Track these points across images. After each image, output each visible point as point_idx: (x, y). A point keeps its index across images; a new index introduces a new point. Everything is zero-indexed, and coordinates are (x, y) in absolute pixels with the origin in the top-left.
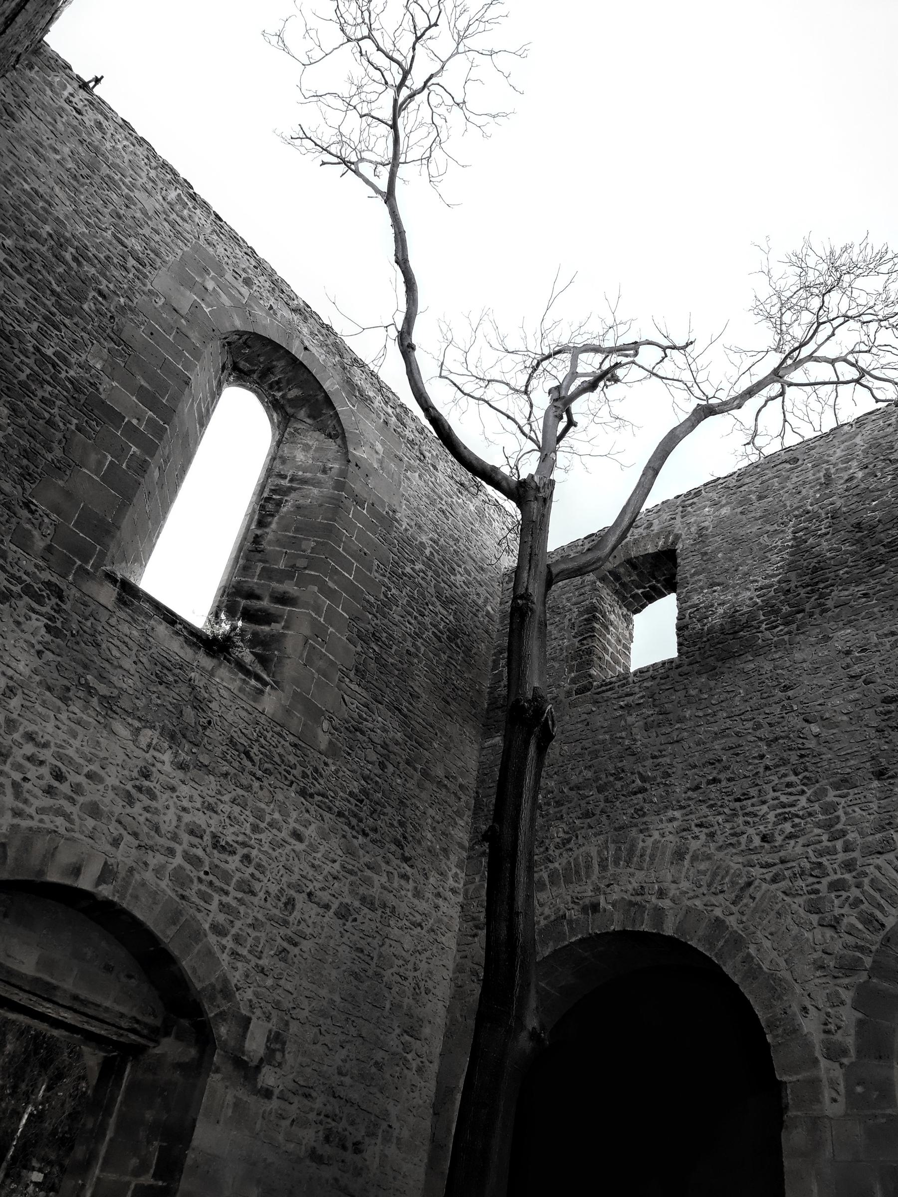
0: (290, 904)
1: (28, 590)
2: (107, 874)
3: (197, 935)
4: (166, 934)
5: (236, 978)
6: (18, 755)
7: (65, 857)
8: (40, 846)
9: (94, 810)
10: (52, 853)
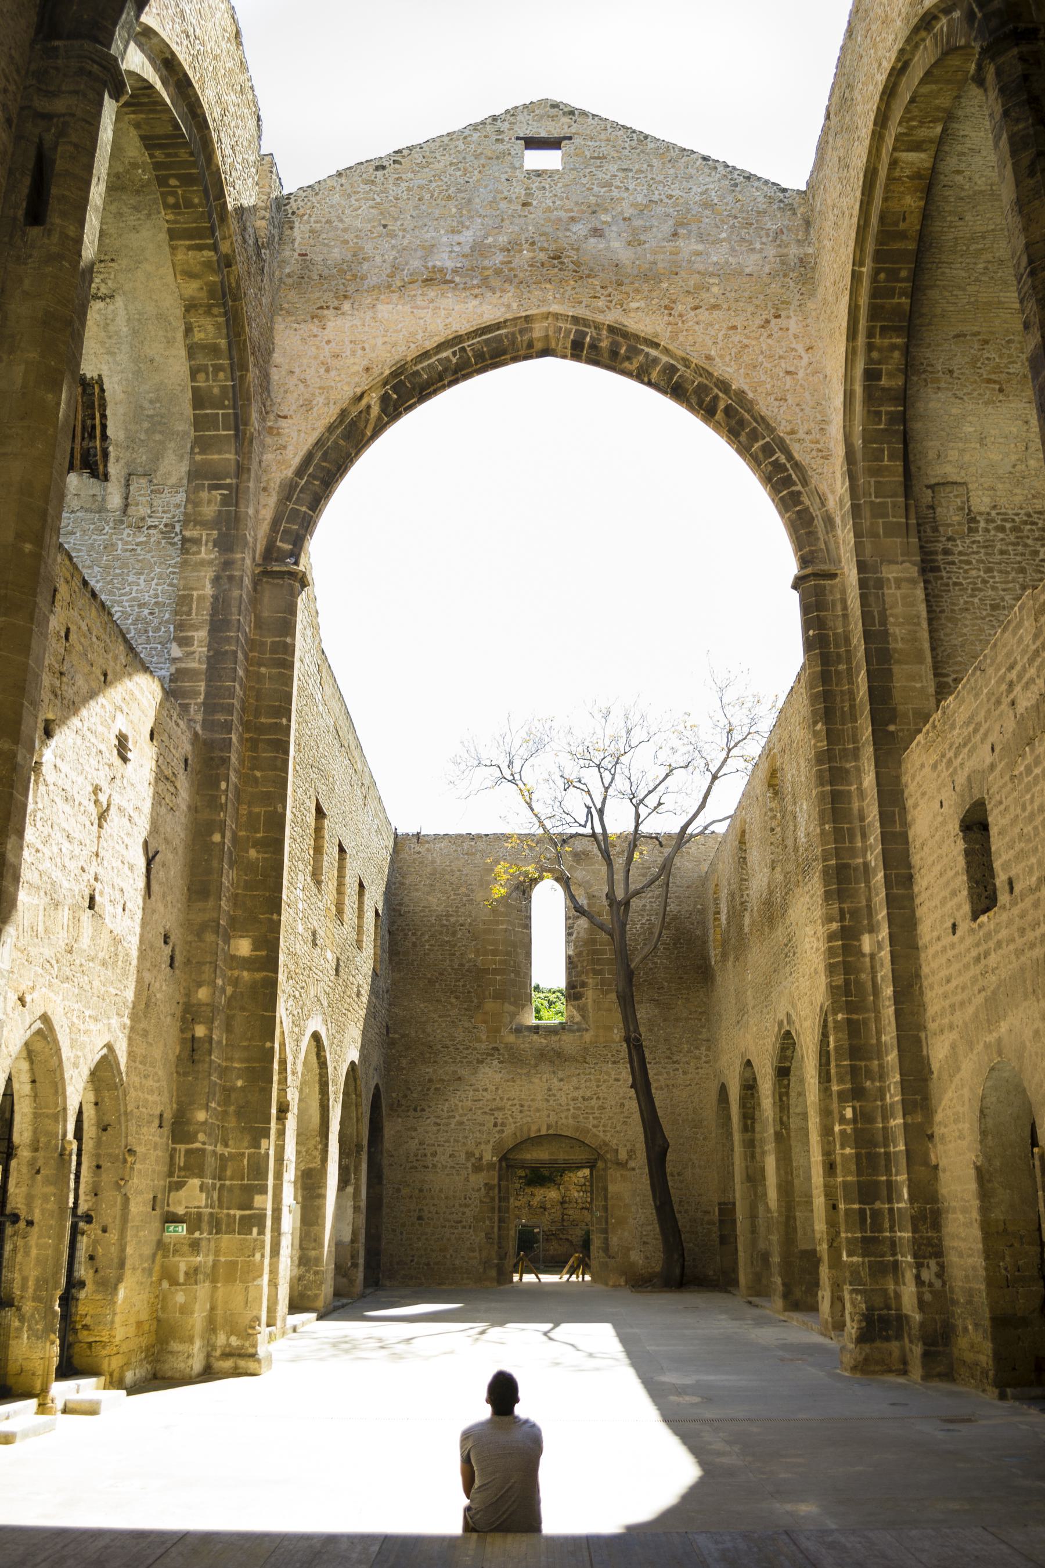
0: (622, 1105)
1: (488, 1054)
2: (549, 1127)
3: (588, 1131)
4: (577, 1135)
5: (607, 1139)
6: (508, 1106)
7: (534, 1128)
8: (525, 1128)
9: (538, 1110)
10: (529, 1130)
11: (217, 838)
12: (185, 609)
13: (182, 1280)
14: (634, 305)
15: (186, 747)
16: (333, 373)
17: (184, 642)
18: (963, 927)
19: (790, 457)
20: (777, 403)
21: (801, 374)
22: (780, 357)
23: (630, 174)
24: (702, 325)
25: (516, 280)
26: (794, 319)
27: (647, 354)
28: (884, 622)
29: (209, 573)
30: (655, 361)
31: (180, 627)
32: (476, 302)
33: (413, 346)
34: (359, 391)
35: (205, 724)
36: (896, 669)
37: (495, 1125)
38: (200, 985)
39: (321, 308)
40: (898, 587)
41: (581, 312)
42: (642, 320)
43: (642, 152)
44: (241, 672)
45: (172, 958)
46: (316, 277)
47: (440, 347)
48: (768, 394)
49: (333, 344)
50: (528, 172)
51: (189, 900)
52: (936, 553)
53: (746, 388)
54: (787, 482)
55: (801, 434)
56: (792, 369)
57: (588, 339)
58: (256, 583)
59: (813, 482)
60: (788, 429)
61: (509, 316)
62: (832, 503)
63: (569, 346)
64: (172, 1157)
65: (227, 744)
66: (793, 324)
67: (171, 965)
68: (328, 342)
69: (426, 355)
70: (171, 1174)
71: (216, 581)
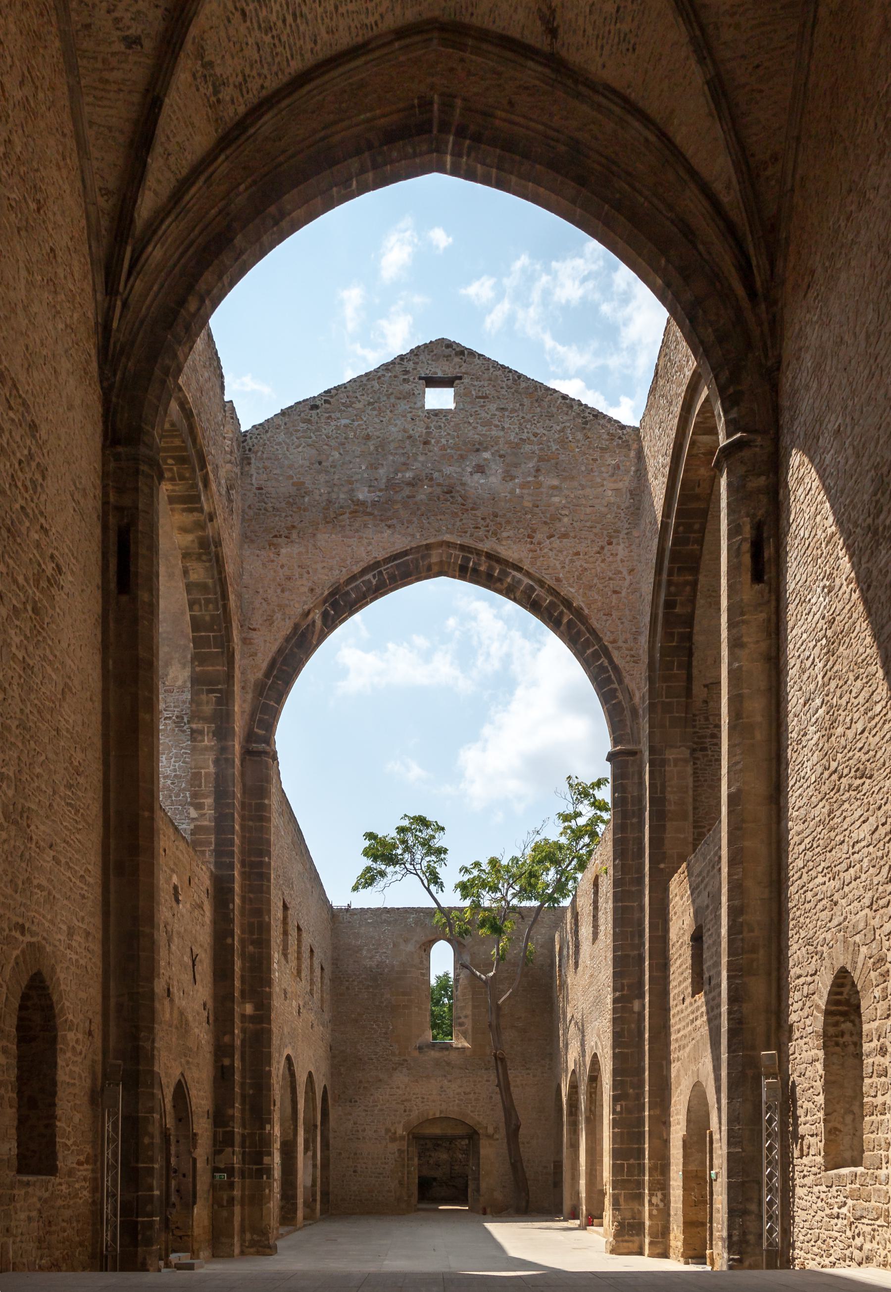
11: (229, 941)
12: (197, 782)
13: (225, 1203)
14: (505, 534)
15: (207, 883)
16: (287, 593)
17: (198, 807)
18: (688, 1000)
19: (611, 661)
20: (604, 618)
21: (624, 594)
22: (610, 579)
23: (506, 413)
24: (555, 552)
25: (419, 513)
26: (620, 548)
27: (514, 576)
28: (663, 792)
29: (210, 757)
30: (520, 582)
31: (195, 795)
32: (389, 532)
33: (344, 570)
34: (306, 607)
35: (217, 865)
36: (669, 825)
37: (405, 1111)
38: (225, 1034)
39: (276, 536)
40: (675, 766)
41: (467, 541)
42: (511, 551)
43: (516, 391)
44: (237, 827)
45: (208, 1017)
46: (271, 509)
47: (364, 572)
48: (599, 611)
49: (286, 568)
50: (429, 411)
51: (215, 980)
52: (705, 737)
53: (583, 605)
54: (609, 680)
55: (620, 643)
56: (618, 589)
57: (471, 564)
58: (243, 761)
59: (627, 680)
60: (612, 638)
61: (414, 545)
62: (637, 699)
63: (457, 569)
64: (215, 1134)
65: (232, 879)
66: (621, 550)
67: (208, 1022)
68: (282, 566)
69: (353, 578)
70: (214, 1145)
71: (217, 762)
